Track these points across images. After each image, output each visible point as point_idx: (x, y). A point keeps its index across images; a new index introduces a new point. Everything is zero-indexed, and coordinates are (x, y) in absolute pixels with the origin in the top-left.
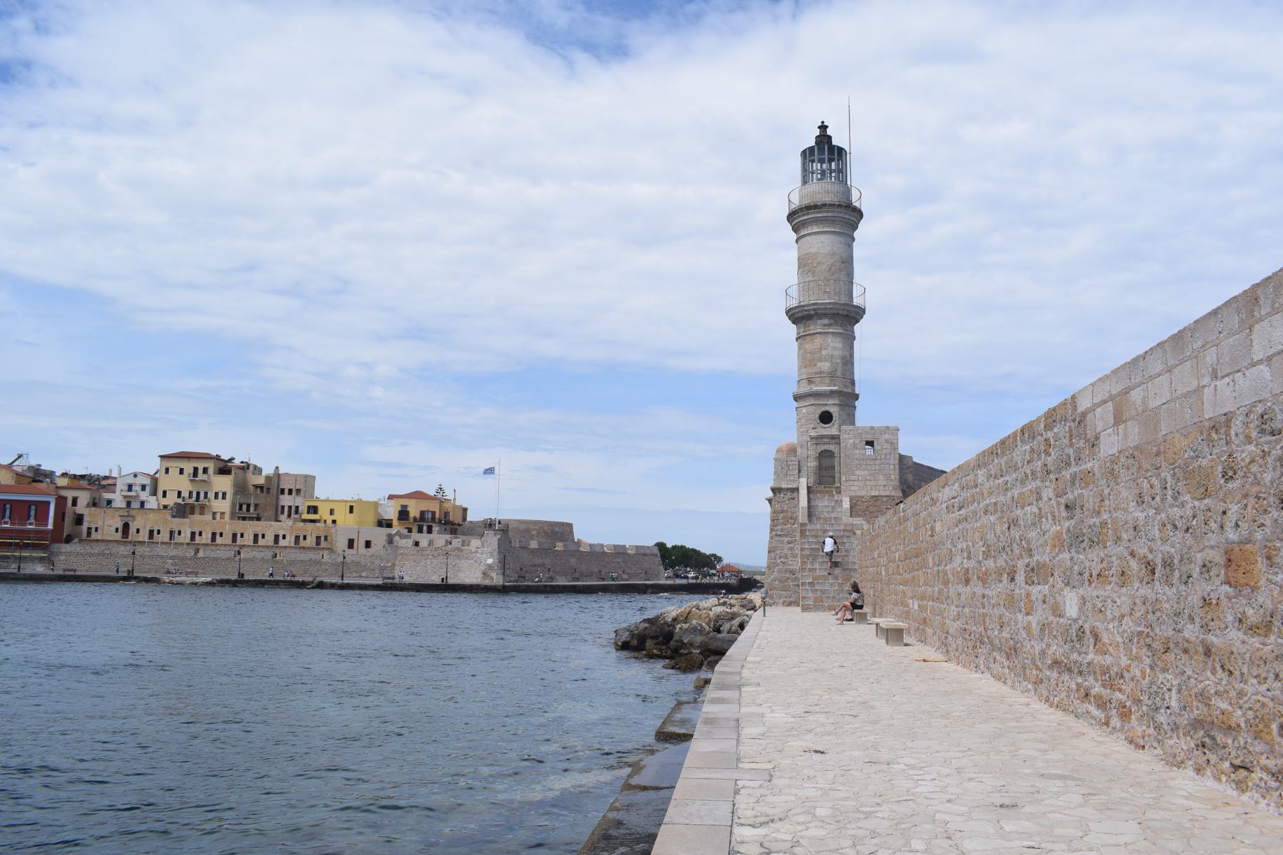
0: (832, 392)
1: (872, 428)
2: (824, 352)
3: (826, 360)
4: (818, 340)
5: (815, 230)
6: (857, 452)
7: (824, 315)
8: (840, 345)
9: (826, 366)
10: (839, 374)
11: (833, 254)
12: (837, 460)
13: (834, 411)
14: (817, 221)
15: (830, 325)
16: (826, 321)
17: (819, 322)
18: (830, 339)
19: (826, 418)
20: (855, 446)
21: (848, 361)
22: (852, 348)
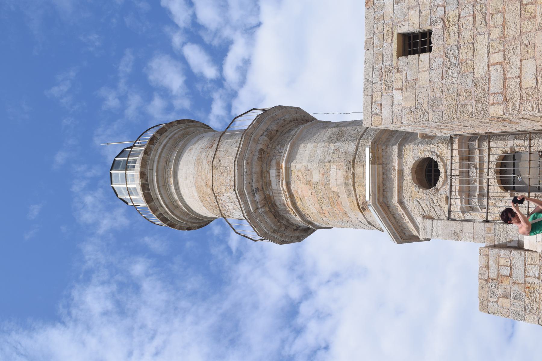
0: (373, 161)
1: (369, 44)
2: (316, 178)
3: (326, 174)
4: (299, 188)
5: (173, 189)
6: (424, 77)
7: (264, 174)
8: (310, 146)
9: (337, 174)
10: (351, 147)
11: (198, 161)
12: (520, 145)
13: (413, 154)
14: (164, 186)
15: (278, 165)
16: (273, 172)
17: (274, 185)
18: (296, 166)
19: (428, 173)
20: (411, 85)
21: (341, 130)
22: (326, 124)
